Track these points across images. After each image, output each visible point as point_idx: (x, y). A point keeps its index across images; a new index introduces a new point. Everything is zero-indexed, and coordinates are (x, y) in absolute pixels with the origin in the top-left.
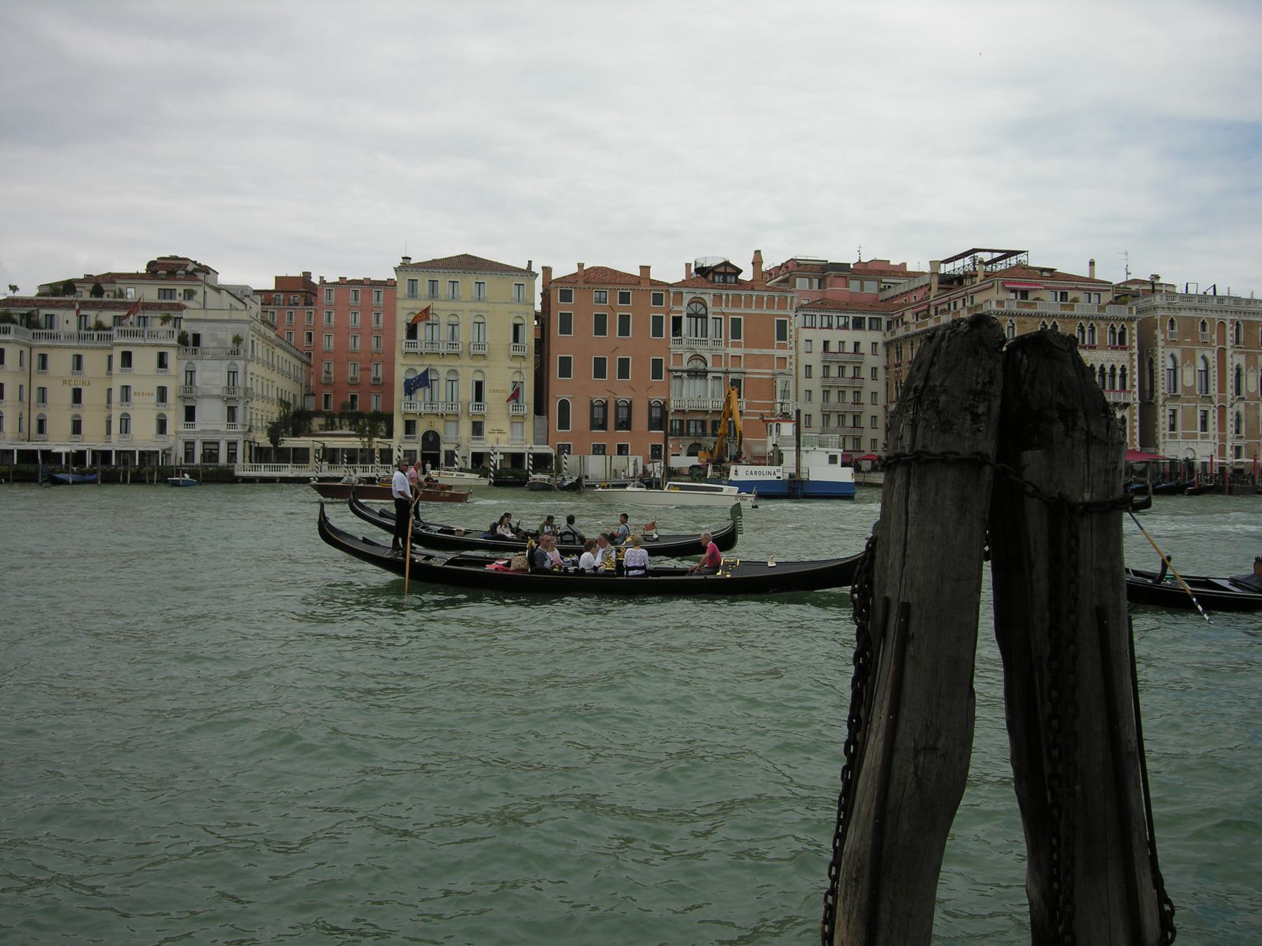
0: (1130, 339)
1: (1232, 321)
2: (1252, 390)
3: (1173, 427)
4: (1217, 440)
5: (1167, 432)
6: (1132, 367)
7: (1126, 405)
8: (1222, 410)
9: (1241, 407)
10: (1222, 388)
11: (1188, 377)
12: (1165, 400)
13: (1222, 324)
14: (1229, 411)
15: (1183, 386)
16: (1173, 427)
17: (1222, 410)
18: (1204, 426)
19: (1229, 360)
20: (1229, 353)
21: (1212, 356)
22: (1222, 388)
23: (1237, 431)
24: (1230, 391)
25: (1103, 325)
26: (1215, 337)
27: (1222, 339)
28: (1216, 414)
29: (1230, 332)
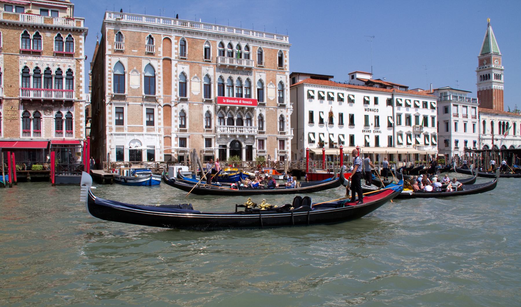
0: (77, 48)
1: (177, 38)
2: (196, 93)
3: (120, 122)
4: (162, 133)
5: (114, 126)
6: (79, 71)
7: (70, 104)
8: (167, 107)
9: (185, 106)
10: (167, 90)
11: (135, 82)
12: (112, 99)
13: (168, 39)
14: (174, 109)
15: (130, 88)
16: (120, 122)
17: (167, 107)
18: (150, 123)
19: (174, 68)
20: (174, 63)
21: (158, 65)
22: (167, 90)
23: (183, 126)
24: (175, 94)
25: (48, 34)
26: (160, 49)
27: (168, 50)
28: (162, 112)
29: (175, 47)
